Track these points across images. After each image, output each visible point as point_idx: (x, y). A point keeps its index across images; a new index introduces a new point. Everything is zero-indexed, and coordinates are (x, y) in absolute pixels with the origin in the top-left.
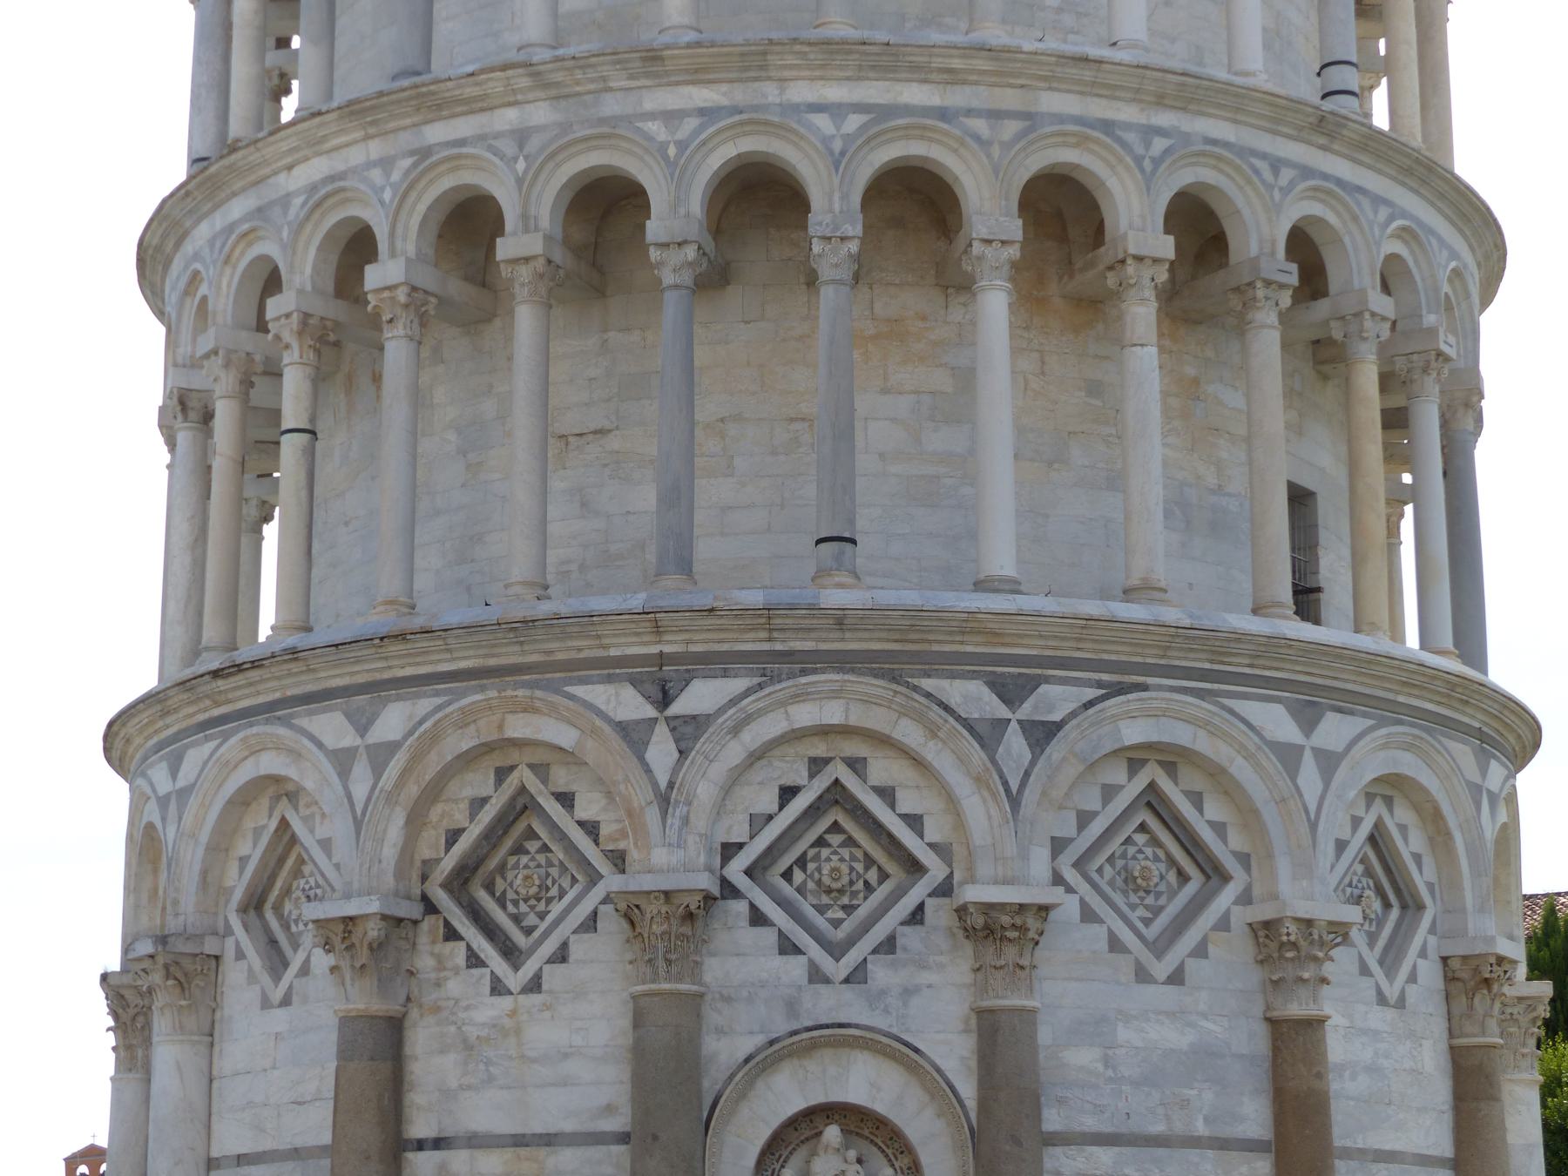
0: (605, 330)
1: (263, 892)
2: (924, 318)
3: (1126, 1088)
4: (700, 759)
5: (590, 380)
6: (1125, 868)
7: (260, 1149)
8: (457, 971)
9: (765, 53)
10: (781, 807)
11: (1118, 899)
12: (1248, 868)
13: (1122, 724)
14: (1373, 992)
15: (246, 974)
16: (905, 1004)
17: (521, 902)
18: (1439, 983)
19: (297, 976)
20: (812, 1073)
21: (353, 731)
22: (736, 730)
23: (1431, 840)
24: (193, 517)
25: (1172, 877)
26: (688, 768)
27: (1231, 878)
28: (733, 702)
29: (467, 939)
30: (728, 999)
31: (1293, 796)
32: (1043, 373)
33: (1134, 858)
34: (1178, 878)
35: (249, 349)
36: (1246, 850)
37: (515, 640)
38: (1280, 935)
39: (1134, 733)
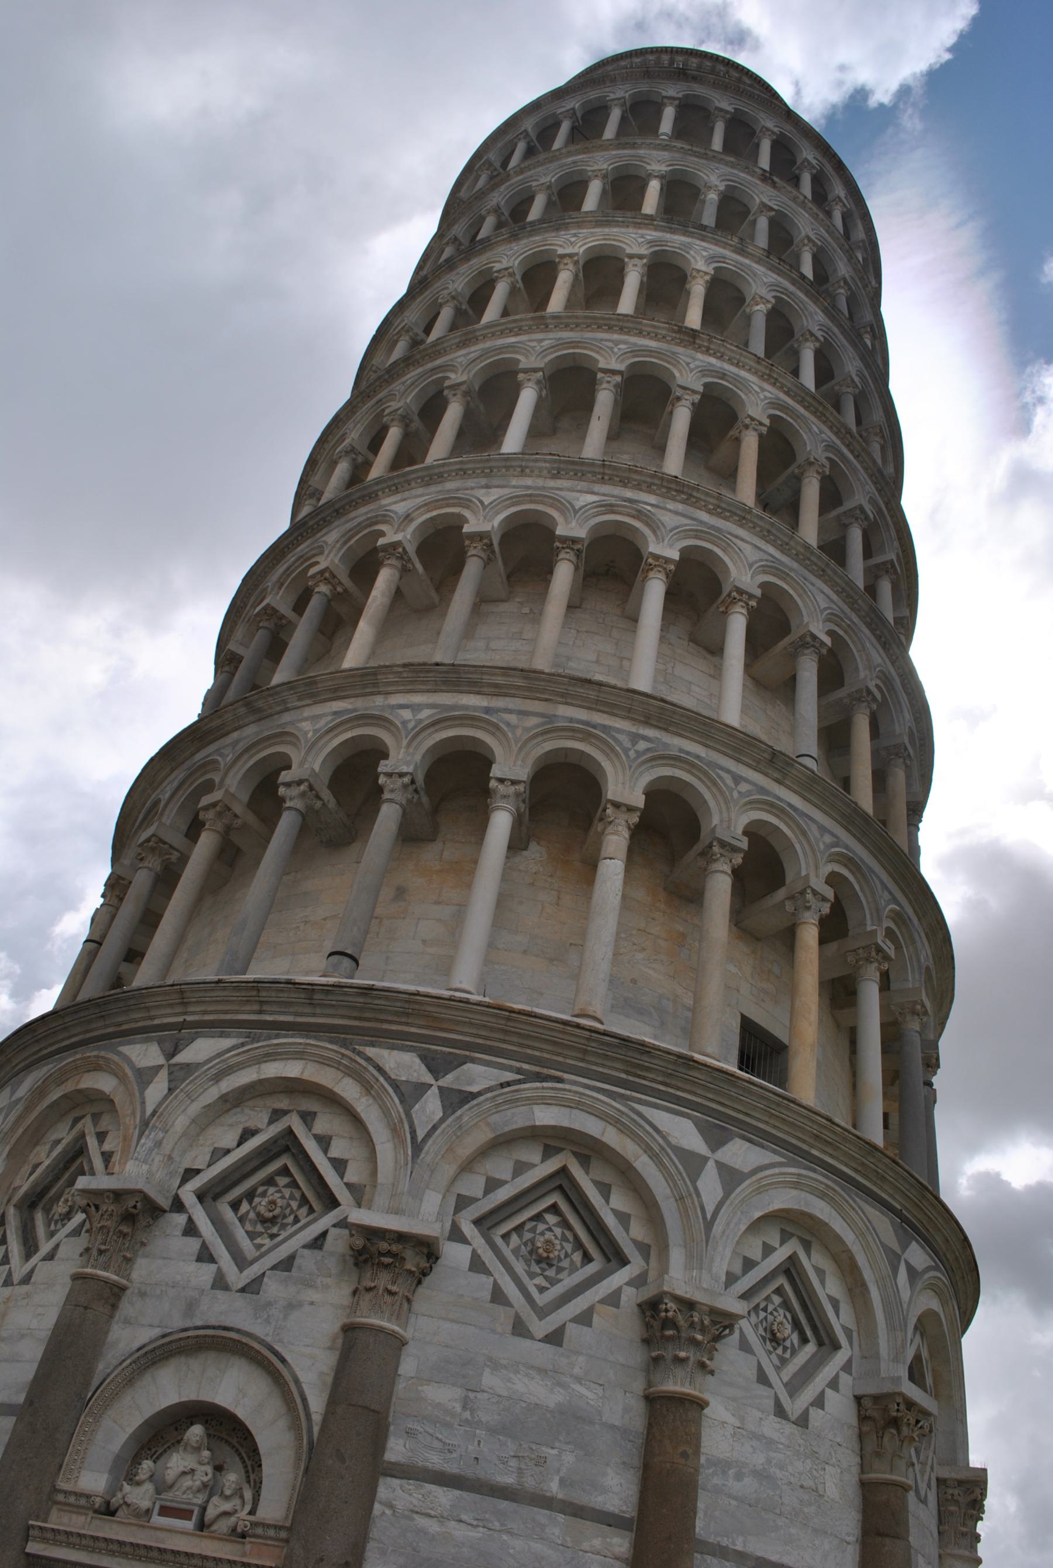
3: (481, 1433)
6: (532, 1241)
9: (375, 674)
10: (239, 1145)
11: (519, 1267)
12: (646, 1257)
13: (536, 1108)
14: (771, 1403)
16: (285, 1317)
18: (854, 1421)
20: (193, 1372)
22: (217, 1078)
23: (850, 1290)
25: (577, 1257)
26: (171, 1101)
27: (629, 1262)
28: (219, 1055)
31: (690, 1195)
32: (558, 904)
34: (583, 1259)
36: (647, 1241)
37: (99, 1015)
38: (660, 1312)
39: (546, 1116)
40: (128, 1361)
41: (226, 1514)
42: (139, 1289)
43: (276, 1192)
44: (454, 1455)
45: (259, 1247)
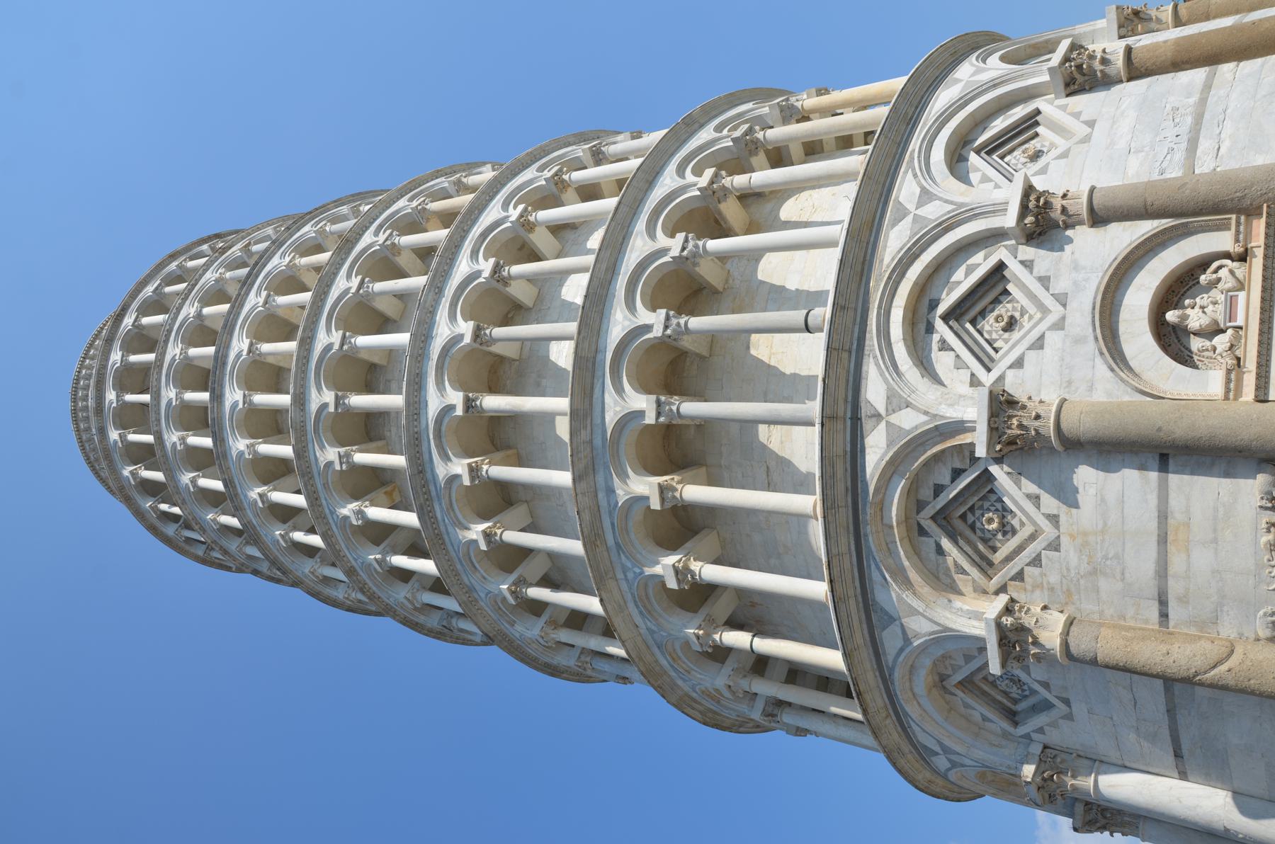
0: (721, 466)
1: (1003, 709)
2: (735, 298)
4: (913, 396)
5: (743, 476)
7: (1169, 738)
8: (1044, 575)
10: (953, 350)
15: (1052, 729)
17: (1005, 529)
19: (1050, 692)
20: (1127, 329)
21: (892, 626)
24: (823, 721)
28: (882, 375)
29: (1023, 565)
30: (1070, 383)
33: (1018, 160)
35: (732, 668)
37: (837, 510)
40: (1121, 374)
41: (1232, 272)
42: (1065, 388)
43: (988, 324)
44: (1175, 146)
45: (1031, 317)
